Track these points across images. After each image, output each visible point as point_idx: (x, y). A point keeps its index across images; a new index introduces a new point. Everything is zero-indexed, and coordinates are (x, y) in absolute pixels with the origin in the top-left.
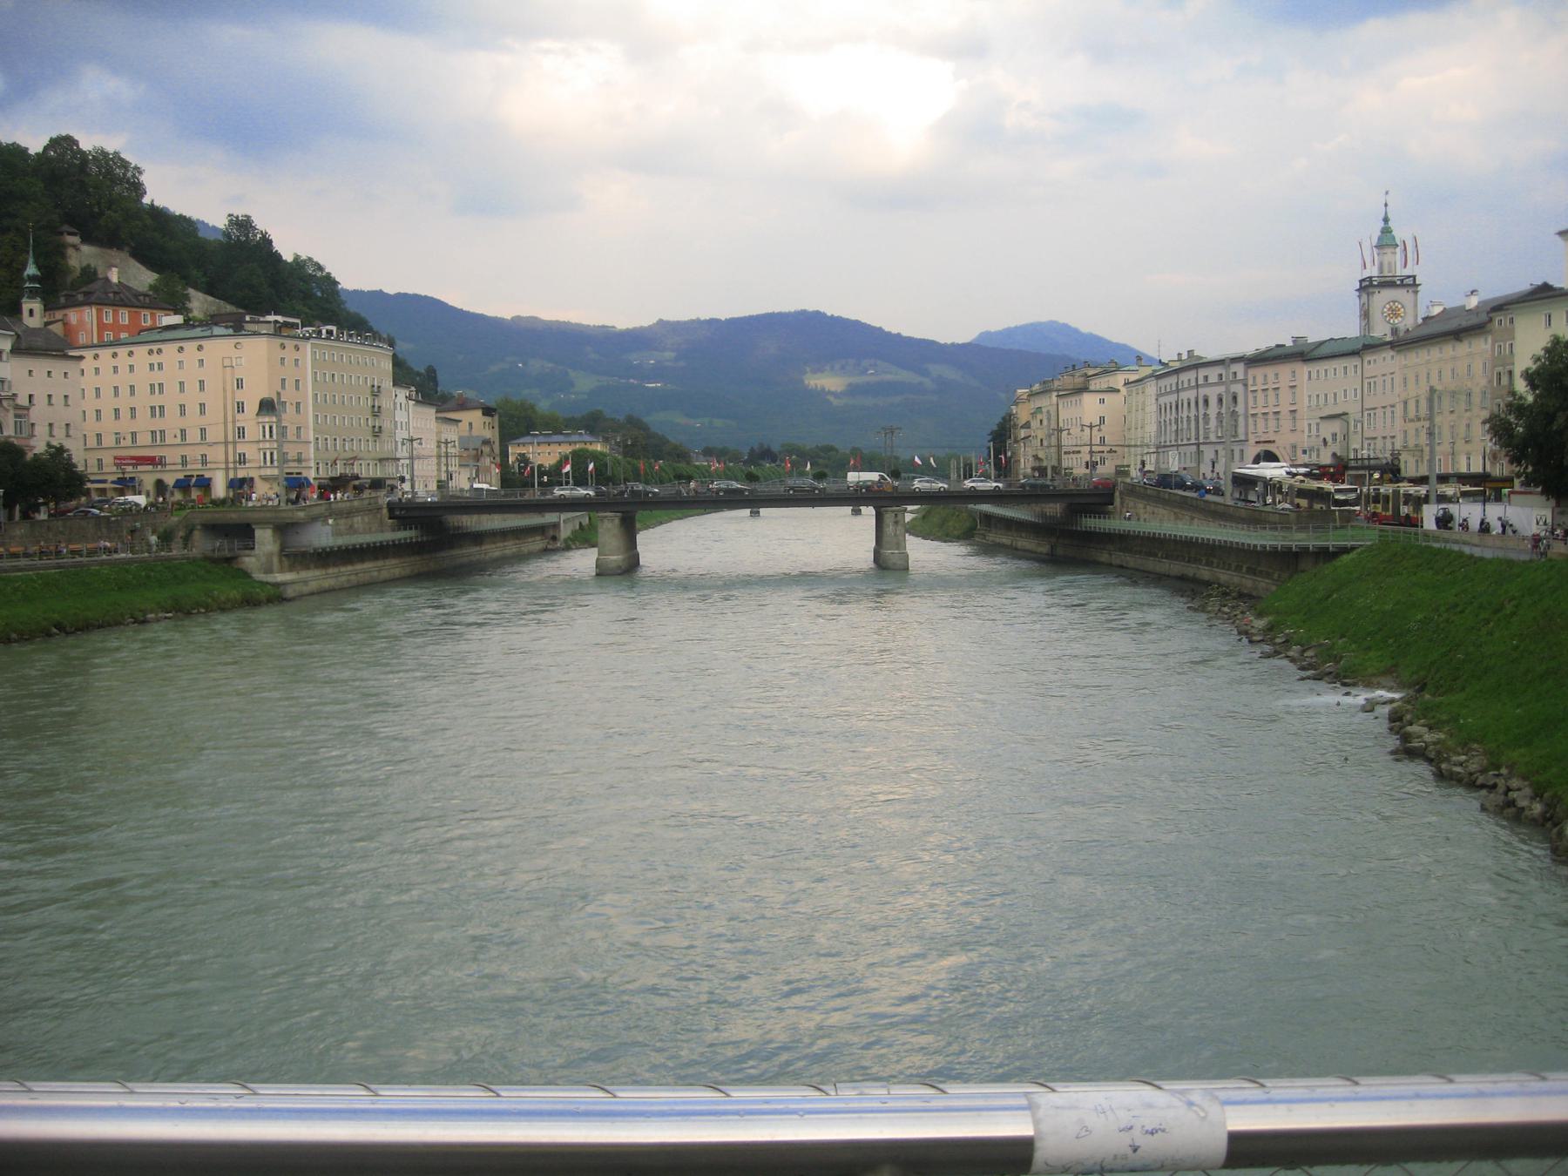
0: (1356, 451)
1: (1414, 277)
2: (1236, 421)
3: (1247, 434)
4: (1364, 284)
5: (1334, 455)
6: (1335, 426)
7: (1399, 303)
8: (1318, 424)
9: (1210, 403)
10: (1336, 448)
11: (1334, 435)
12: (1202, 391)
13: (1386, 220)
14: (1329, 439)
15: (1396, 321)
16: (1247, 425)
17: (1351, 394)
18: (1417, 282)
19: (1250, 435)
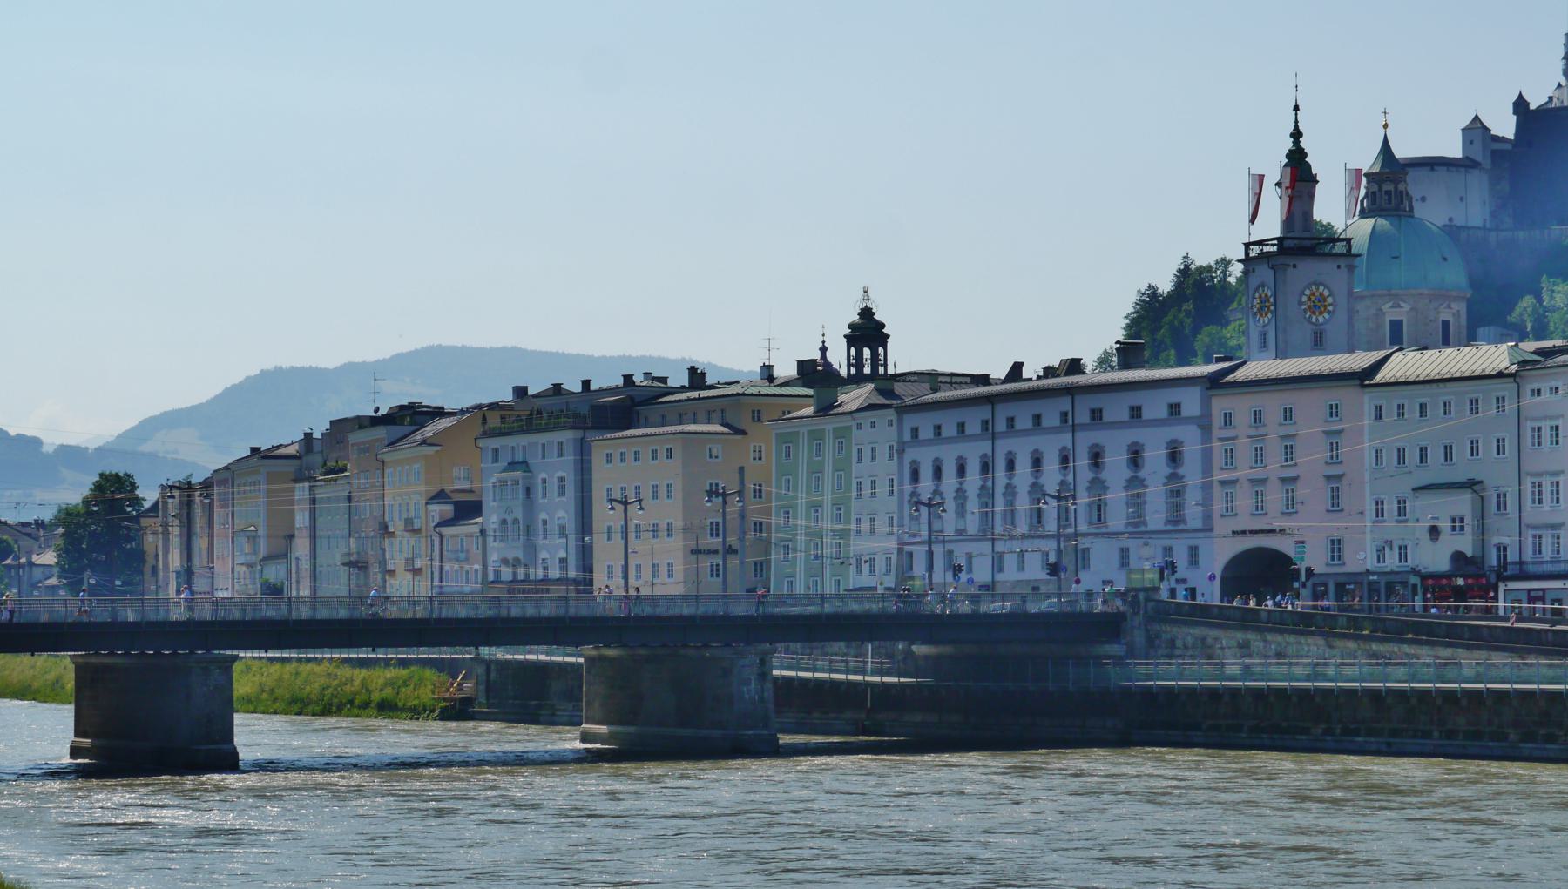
0: (1502, 549)
1: (1349, 240)
2: (1178, 493)
3: (1208, 517)
4: (1254, 251)
5: (1458, 557)
6: (1463, 504)
7: (1326, 287)
8: (1401, 502)
9: (1017, 465)
10: (1466, 544)
11: (1457, 524)
12: (1085, 440)
13: (1297, 135)
14: (1445, 525)
15: (1321, 319)
16: (1207, 501)
17: (1488, 449)
18: (1354, 251)
19: (1216, 516)
